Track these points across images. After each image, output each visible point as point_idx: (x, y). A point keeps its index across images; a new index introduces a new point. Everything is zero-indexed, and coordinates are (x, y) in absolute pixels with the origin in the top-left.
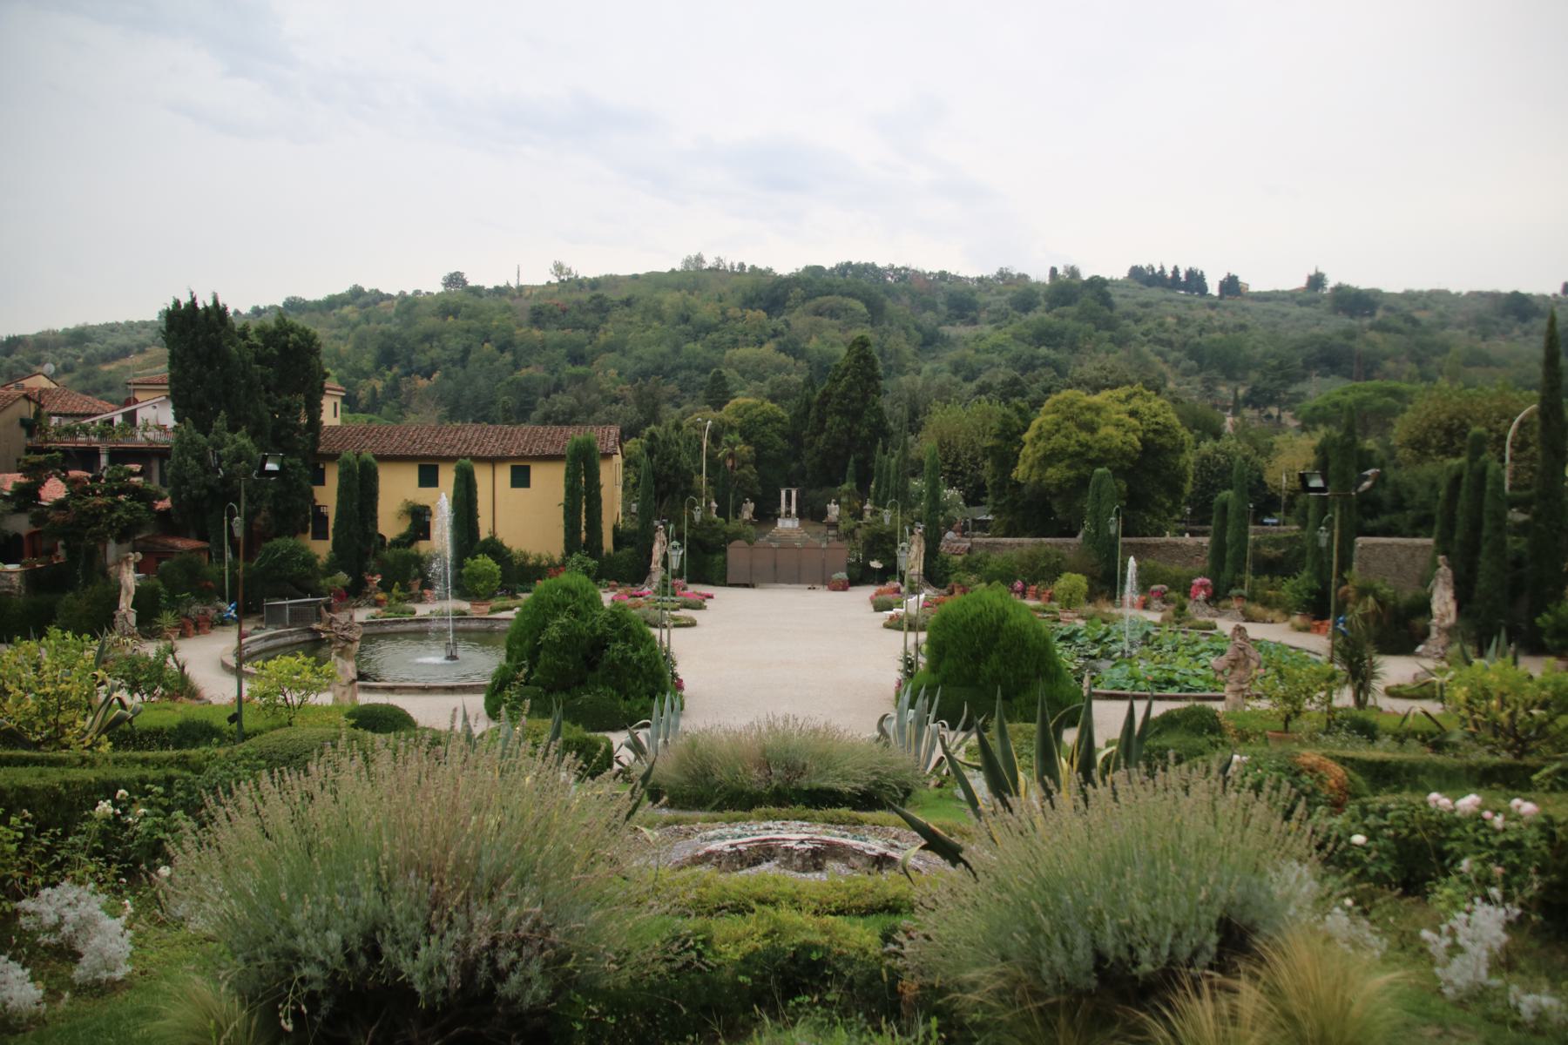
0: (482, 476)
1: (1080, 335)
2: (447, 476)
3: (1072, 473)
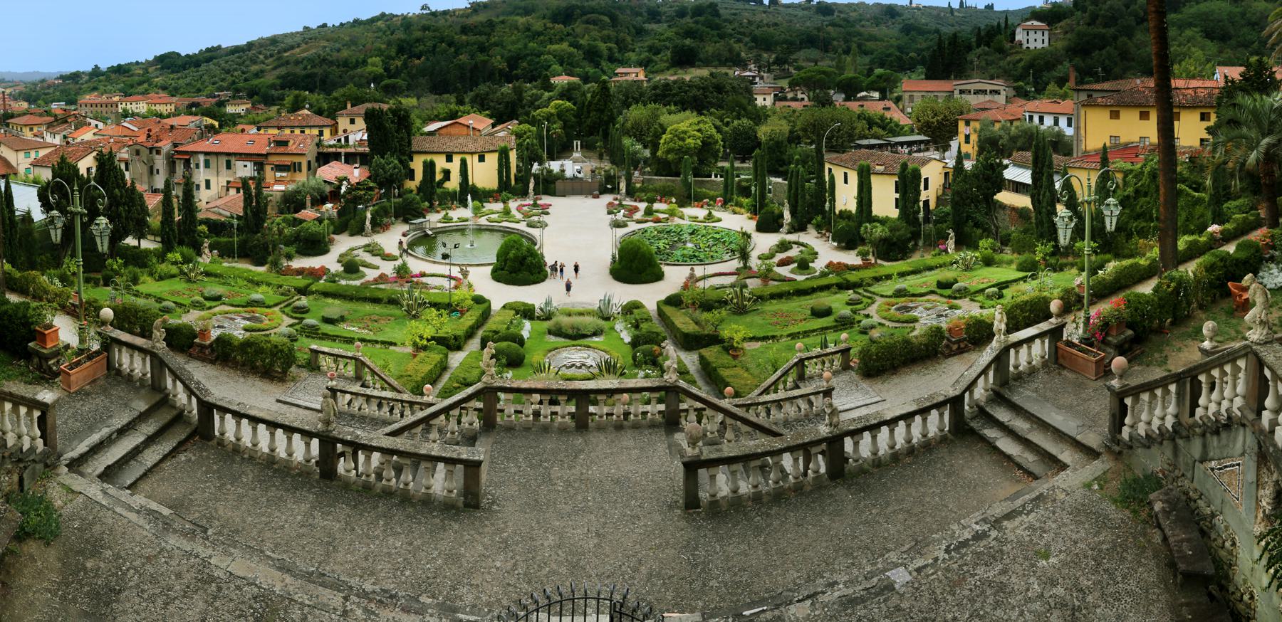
0: (468, 158)
2: (457, 159)
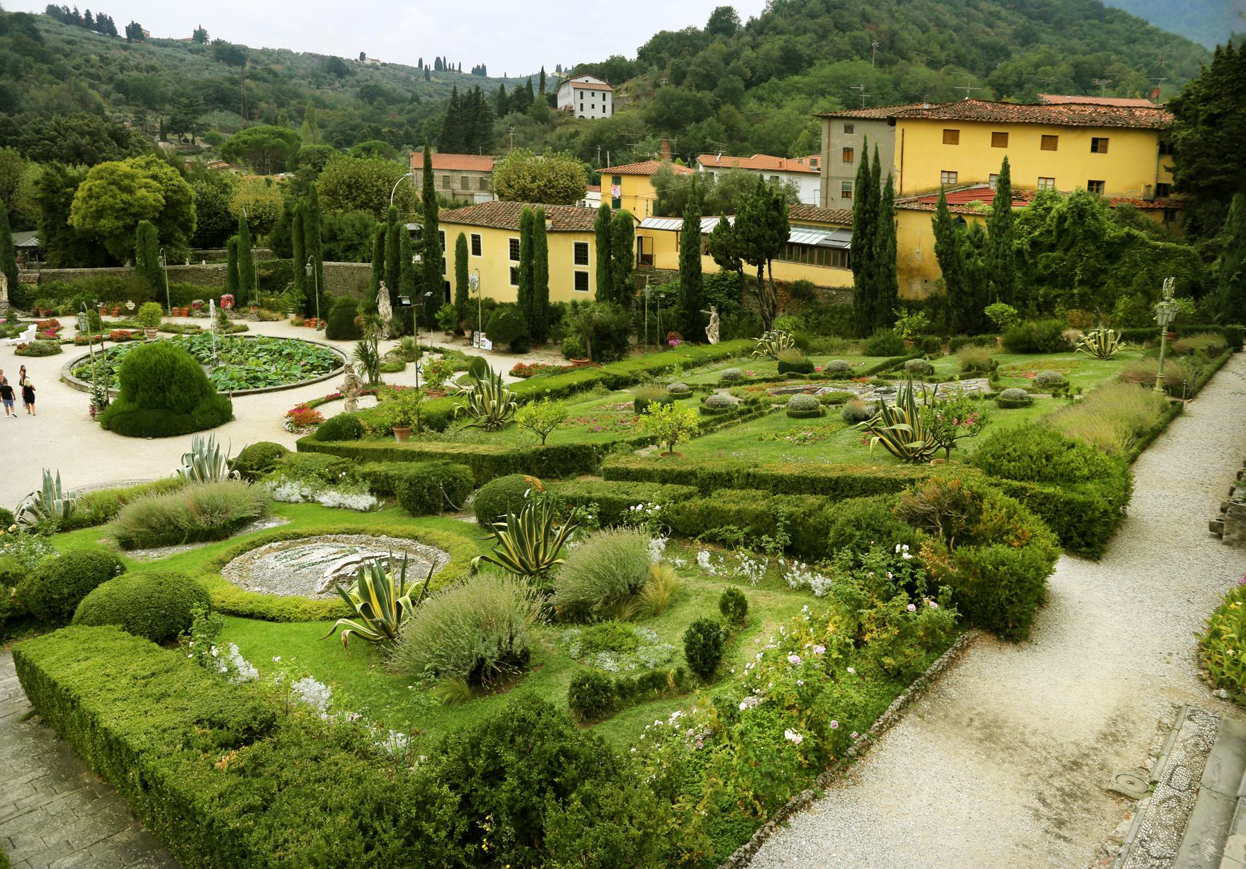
1: (22, 66)
3: (120, 223)
